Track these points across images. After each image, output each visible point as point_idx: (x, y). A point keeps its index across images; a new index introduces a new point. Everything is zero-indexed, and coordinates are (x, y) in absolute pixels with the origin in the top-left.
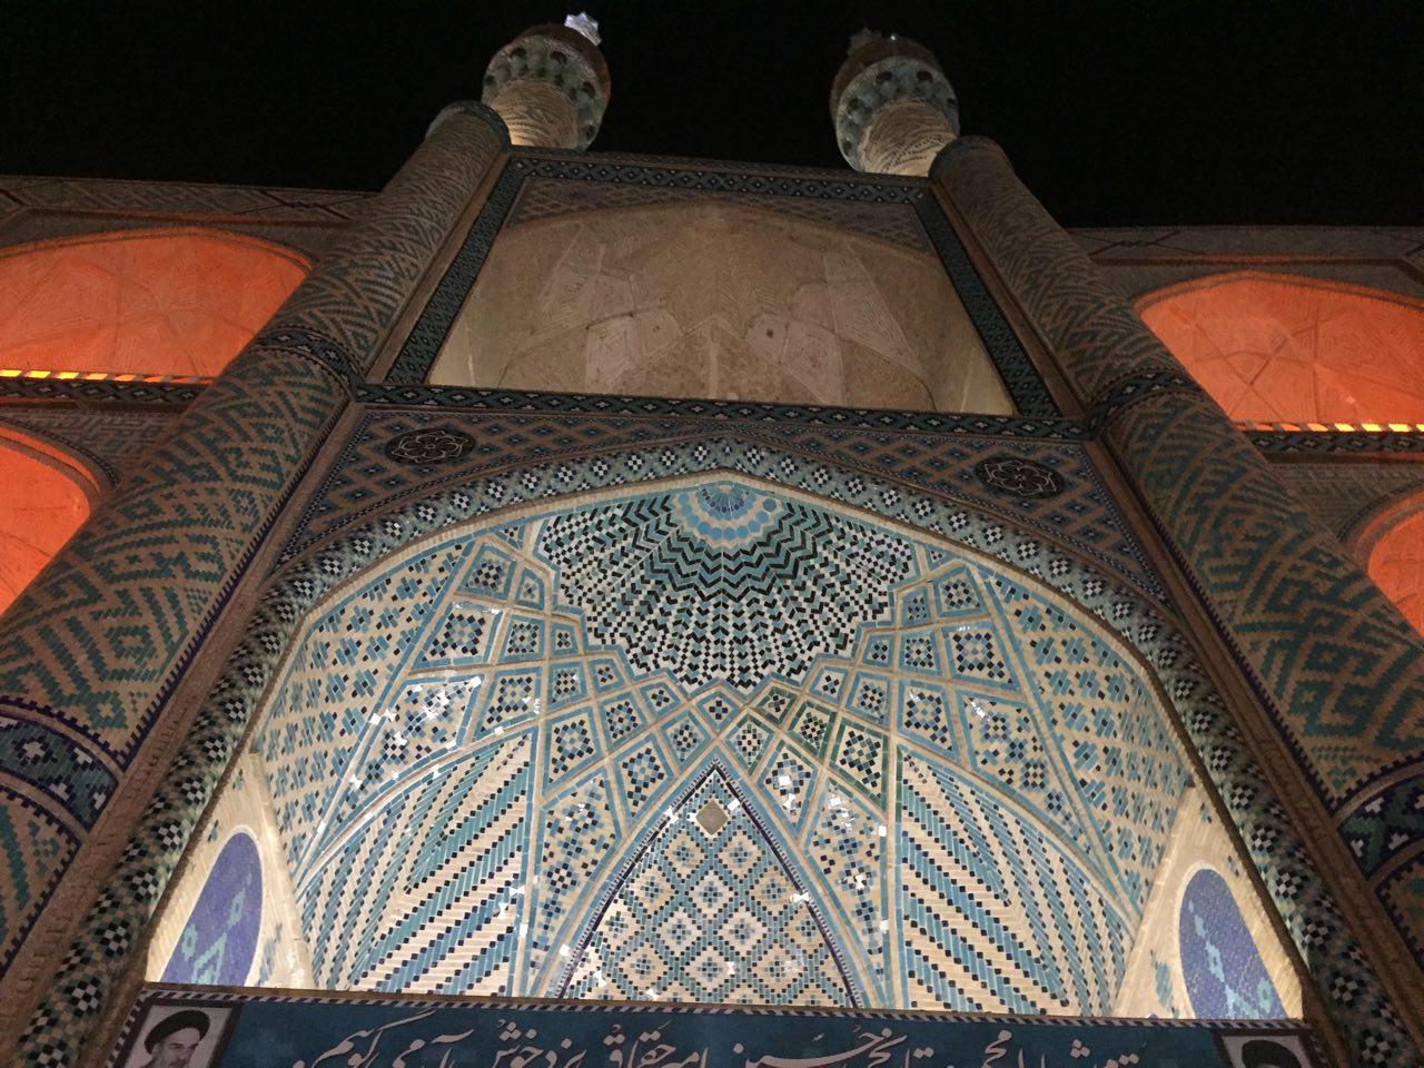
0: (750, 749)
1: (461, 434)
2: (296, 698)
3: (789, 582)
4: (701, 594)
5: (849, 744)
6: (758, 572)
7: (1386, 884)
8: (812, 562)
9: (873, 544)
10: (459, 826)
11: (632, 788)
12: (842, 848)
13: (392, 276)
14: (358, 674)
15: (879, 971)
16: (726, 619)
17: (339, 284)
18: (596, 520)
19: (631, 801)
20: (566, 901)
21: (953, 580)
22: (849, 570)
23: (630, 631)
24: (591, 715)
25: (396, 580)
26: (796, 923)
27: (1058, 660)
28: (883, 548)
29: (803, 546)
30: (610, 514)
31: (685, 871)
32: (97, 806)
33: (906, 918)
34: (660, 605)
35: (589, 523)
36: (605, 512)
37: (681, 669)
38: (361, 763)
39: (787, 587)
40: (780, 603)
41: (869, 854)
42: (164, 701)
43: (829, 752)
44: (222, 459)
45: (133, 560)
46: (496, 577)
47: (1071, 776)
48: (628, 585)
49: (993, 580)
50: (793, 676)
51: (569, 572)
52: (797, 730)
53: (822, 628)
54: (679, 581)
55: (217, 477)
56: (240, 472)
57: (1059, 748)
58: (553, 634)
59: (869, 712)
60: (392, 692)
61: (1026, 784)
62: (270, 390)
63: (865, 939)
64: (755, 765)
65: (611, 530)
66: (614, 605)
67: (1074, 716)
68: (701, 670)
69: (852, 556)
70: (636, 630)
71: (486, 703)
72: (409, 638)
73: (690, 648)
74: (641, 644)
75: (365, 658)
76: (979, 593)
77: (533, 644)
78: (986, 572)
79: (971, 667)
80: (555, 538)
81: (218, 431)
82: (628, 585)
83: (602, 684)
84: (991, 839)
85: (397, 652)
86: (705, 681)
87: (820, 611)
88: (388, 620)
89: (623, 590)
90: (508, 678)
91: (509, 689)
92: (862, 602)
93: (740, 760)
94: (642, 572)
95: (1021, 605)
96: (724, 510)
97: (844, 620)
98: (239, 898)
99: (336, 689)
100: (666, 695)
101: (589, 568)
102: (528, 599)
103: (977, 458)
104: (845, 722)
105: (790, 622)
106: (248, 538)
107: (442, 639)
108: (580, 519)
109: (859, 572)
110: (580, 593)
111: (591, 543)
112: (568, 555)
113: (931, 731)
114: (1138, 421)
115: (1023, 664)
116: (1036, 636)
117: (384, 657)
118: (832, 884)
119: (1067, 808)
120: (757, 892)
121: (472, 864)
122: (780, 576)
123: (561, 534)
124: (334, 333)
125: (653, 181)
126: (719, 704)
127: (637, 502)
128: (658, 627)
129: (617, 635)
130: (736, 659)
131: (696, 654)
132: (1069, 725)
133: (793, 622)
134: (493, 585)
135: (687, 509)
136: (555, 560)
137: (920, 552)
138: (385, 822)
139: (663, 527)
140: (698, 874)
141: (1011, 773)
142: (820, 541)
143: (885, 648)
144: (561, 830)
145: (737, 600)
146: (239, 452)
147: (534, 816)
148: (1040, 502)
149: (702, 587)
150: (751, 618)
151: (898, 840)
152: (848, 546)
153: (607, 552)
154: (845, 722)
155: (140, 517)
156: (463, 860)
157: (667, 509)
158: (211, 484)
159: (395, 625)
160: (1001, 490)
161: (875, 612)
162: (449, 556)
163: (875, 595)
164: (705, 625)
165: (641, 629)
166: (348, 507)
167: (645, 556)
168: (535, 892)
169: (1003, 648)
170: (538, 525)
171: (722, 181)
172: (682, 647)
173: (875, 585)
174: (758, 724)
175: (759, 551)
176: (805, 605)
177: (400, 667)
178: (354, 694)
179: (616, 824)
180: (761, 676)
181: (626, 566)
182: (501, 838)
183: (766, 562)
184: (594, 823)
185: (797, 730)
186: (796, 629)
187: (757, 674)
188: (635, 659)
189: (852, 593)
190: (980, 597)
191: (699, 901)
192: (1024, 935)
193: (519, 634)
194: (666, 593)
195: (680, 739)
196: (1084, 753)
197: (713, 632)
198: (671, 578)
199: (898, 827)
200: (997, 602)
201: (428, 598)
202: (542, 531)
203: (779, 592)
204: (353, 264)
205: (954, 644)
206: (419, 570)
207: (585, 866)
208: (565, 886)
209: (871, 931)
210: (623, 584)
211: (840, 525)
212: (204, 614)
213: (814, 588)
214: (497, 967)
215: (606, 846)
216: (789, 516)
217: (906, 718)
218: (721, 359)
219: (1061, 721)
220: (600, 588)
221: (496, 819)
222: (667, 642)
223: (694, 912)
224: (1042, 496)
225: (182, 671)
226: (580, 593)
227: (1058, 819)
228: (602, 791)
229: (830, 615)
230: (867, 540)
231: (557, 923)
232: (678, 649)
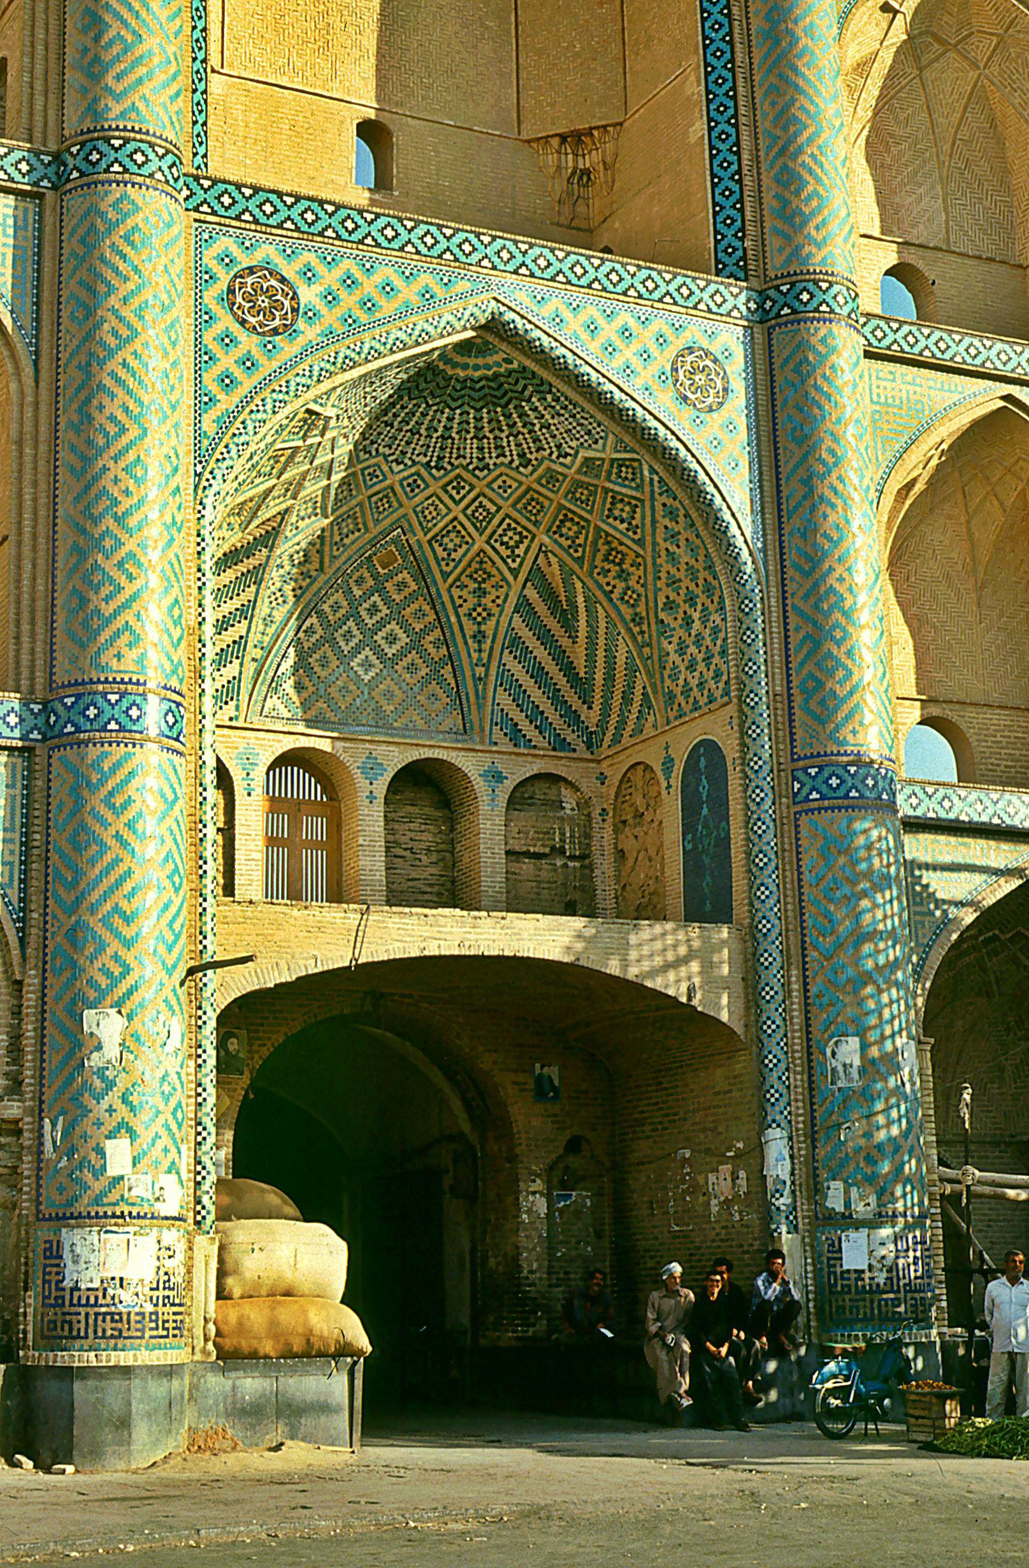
1: (283, 280)
6: (476, 395)
7: (800, 813)
11: (337, 538)
31: (358, 593)
43: (489, 531)
47: (656, 614)
49: (656, 478)
52: (469, 512)
63: (475, 655)
64: (430, 530)
69: (559, 415)
78: (653, 471)
79: (615, 519)
87: (516, 436)
115: (654, 534)
128: (386, 424)
131: (408, 443)
140: (367, 595)
154: (508, 516)
166: (226, 402)
169: (643, 517)
179: (322, 563)
185: (469, 512)
191: (363, 613)
200: (652, 492)
209: (480, 651)
219: (664, 580)
223: (360, 622)
224: (711, 410)
227: (636, 629)
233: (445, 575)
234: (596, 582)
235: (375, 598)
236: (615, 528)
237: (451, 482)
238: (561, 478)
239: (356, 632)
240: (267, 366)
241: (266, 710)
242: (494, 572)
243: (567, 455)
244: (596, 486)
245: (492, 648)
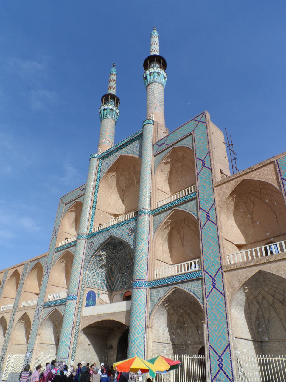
20: (124, 275)
25: (93, 262)
103: (129, 228)
168: (121, 276)
218: (134, 175)
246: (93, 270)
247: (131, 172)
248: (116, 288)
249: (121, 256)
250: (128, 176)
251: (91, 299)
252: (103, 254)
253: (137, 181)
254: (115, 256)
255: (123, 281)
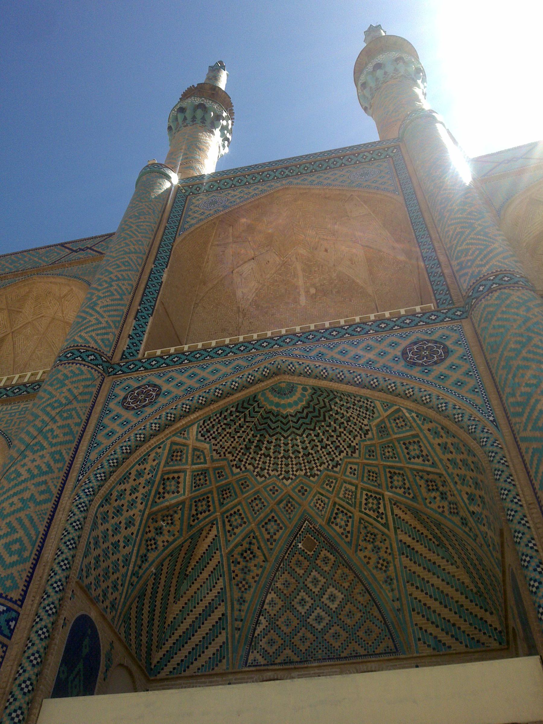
0: (321, 508)
1: (155, 386)
2: (96, 543)
3: (323, 424)
4: (283, 436)
5: (366, 499)
6: (307, 421)
8: (331, 413)
9: (356, 402)
10: (192, 569)
11: (268, 536)
12: (373, 551)
13: (118, 297)
14: (126, 519)
15: (398, 610)
16: (298, 446)
17: (93, 313)
18: (223, 416)
19: (269, 543)
20: (248, 596)
21: (397, 416)
22: (348, 415)
23: (253, 461)
24: (242, 506)
25: (133, 472)
26: (357, 591)
27: (451, 453)
28: (361, 403)
29: (325, 406)
30: (229, 411)
32: (12, 627)
33: (408, 582)
34: (265, 445)
35: (220, 418)
36: (226, 411)
37: (281, 474)
38: (137, 556)
39: (323, 426)
40: (321, 434)
41: (386, 552)
42: (34, 569)
44: (46, 438)
45: (12, 504)
46: (181, 456)
47: (468, 508)
48: (247, 440)
49: (414, 415)
50: (335, 469)
51: (216, 442)
52: (341, 496)
53: (343, 444)
54: (271, 432)
55: (43, 448)
56: (54, 441)
57: (461, 496)
58: (215, 473)
59: (372, 483)
60: (144, 522)
61: (451, 512)
62: (65, 390)
63: (390, 594)
65: (232, 418)
66: (242, 451)
67: (464, 480)
68: (291, 473)
70: (256, 460)
71: (189, 514)
72: (146, 496)
73: (283, 463)
74: (260, 466)
75: (127, 511)
76: (409, 421)
77: (206, 480)
78: (410, 411)
80: (205, 430)
81: (43, 421)
82: (247, 440)
83: (244, 490)
84: (443, 539)
85: (142, 503)
86: (294, 477)
87: (340, 436)
88: (134, 490)
89: (245, 443)
90: (197, 500)
91: (199, 504)
92: (358, 430)
93: (317, 514)
94: (252, 432)
95: (430, 426)
96: (285, 394)
97: (352, 439)
98: (86, 642)
99: (116, 529)
100: (276, 488)
101: (226, 438)
102: (198, 461)
103: (404, 344)
104: (363, 489)
105: (327, 442)
106: (62, 474)
107: (161, 491)
108: (215, 418)
109: (353, 415)
110: (224, 450)
111: (224, 426)
112: (214, 435)
113: (403, 490)
114: (484, 308)
116: (439, 441)
117: (136, 507)
118: (371, 568)
119: (469, 524)
120: (337, 577)
121: (201, 586)
122: (318, 421)
123: (208, 427)
124: (93, 344)
125: (252, 182)
126: (302, 488)
127: (241, 403)
128: (266, 456)
129: (247, 465)
130: (306, 464)
131: (287, 465)
132: (463, 484)
133: (329, 443)
134: (180, 460)
135: (267, 399)
136: (208, 439)
137: (378, 404)
138: (154, 579)
139: (257, 409)
141: (443, 507)
142: (332, 403)
143: (373, 452)
144: (239, 563)
145: (301, 436)
146: (52, 430)
147: (225, 559)
148: (435, 367)
149: (283, 433)
150: (309, 443)
151: (397, 544)
152: (345, 404)
153: (233, 428)
155: (13, 479)
156: (196, 585)
157: (257, 401)
158: (41, 453)
159: (138, 491)
160: (414, 364)
161: (365, 434)
162: (157, 453)
163: (363, 426)
164: (288, 450)
165: (258, 459)
166: (106, 442)
167: (251, 425)
170: (195, 427)
171: (287, 172)
172: (280, 463)
173: (362, 421)
174: (322, 495)
175: (305, 411)
176: (333, 434)
177: (145, 509)
178: (126, 528)
179: (264, 555)
180: (320, 471)
181: (243, 432)
182: (212, 572)
183: (310, 415)
184: (254, 556)
185: (341, 496)
186: (331, 446)
187: (318, 470)
188: (258, 474)
189: (353, 426)
190: (411, 423)
191: (310, 585)
192: (467, 581)
193: (198, 478)
194: (266, 440)
195: (287, 508)
196: (471, 498)
197: (293, 453)
198: (267, 432)
199: (397, 539)
201: (150, 475)
202: (198, 428)
203: (320, 429)
204: (99, 298)
205: (404, 447)
206: (143, 464)
207: (253, 578)
208: (246, 589)
210: (244, 441)
211: (339, 395)
212: (46, 520)
213: (335, 425)
214: (220, 633)
215: (261, 567)
216: (315, 393)
217: (390, 485)
218: (304, 270)
220: (233, 445)
221: (208, 563)
222: (272, 462)
224: (435, 363)
225: (40, 552)
226: (224, 450)
227: (467, 530)
228: (254, 541)
229: (345, 437)
230: (353, 400)
231: (245, 607)
232: (278, 464)
233: (349, 543)
234: (431, 509)
235: (314, 573)
236: (417, 464)
237: (324, 482)
238: (373, 448)
239: (308, 599)
240: (134, 420)
241: (249, 661)
242: (376, 531)
243: (367, 431)
244: (391, 441)
245: (398, 585)
246: (118, 511)
247: (294, 259)
248: (177, 659)
249: (274, 491)
250: (273, 272)
251: (80, 666)
252: (198, 444)
253: (313, 291)
254: (244, 484)
255: (239, 624)
